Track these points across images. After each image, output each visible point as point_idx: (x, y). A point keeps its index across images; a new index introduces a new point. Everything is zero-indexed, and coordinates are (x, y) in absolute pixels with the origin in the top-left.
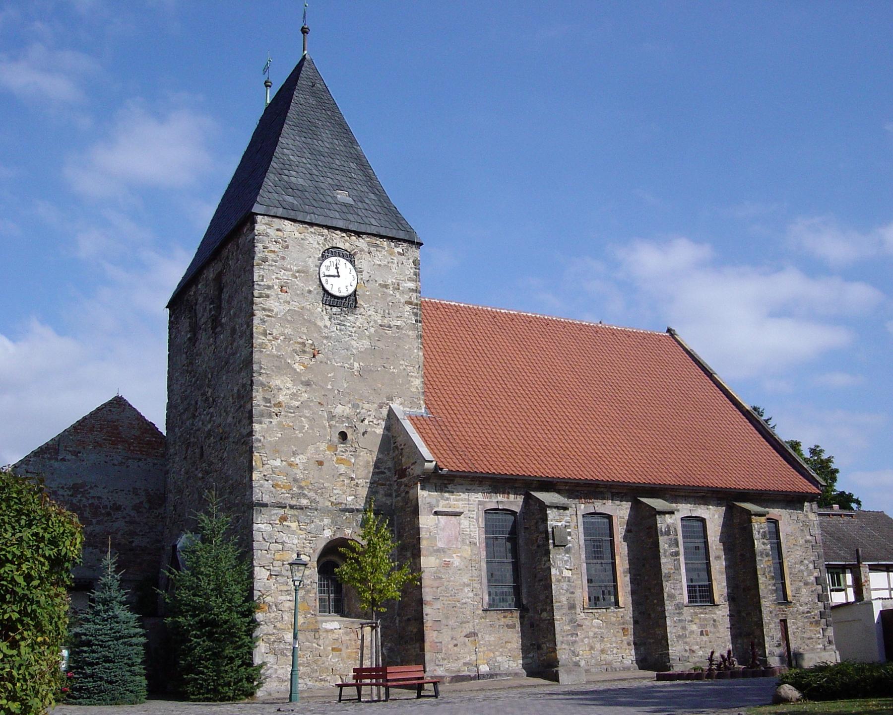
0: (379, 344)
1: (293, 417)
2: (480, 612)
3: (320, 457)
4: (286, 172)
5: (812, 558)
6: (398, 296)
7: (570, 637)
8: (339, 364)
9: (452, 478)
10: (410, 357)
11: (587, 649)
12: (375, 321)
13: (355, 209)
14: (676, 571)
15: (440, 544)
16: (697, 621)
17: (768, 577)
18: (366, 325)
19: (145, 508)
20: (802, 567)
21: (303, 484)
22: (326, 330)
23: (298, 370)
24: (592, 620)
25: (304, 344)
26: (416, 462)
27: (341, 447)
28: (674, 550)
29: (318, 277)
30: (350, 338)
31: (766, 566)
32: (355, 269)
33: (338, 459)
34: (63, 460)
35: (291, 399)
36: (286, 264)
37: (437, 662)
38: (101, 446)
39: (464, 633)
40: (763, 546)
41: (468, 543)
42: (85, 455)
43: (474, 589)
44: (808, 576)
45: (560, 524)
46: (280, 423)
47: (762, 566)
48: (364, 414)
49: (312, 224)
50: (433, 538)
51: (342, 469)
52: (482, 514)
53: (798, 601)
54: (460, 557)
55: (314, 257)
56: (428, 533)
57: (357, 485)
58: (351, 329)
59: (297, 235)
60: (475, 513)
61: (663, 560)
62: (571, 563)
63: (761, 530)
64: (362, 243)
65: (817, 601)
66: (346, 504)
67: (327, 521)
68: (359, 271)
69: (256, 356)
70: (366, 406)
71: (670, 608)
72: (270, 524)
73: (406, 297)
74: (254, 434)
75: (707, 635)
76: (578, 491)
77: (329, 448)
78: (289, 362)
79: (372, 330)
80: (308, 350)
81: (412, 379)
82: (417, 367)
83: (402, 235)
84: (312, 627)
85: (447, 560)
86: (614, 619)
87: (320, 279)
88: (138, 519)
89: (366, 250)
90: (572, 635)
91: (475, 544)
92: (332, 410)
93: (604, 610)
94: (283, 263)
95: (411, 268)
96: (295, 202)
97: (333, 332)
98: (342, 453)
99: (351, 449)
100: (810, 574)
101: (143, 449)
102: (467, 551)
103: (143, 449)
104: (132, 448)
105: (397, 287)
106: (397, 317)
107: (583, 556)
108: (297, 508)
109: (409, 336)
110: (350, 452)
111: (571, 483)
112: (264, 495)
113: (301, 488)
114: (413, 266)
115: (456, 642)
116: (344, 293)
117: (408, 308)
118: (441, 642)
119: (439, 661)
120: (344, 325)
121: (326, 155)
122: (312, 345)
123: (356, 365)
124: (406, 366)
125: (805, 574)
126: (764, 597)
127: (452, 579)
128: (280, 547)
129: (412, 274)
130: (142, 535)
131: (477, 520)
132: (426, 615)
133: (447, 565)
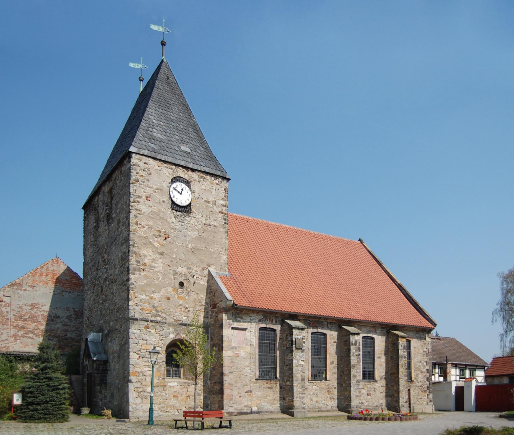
0: (204, 235)
1: (153, 272)
2: (254, 380)
3: (168, 295)
5: (426, 360)
6: (215, 208)
8: (180, 244)
9: (242, 310)
10: (221, 243)
11: (309, 400)
12: (202, 222)
15: (234, 345)
16: (366, 388)
18: (196, 223)
20: (421, 364)
21: (158, 309)
22: (173, 224)
23: (156, 246)
24: (313, 386)
25: (160, 232)
26: (222, 300)
27: (180, 290)
28: (358, 353)
30: (187, 230)
32: (191, 190)
33: (178, 297)
35: (152, 262)
37: (230, 405)
39: (245, 391)
41: (249, 344)
43: (252, 369)
44: (423, 368)
45: (299, 337)
46: (145, 275)
48: (194, 273)
50: (230, 341)
51: (181, 302)
52: (257, 330)
53: (417, 380)
54: (245, 352)
56: (228, 339)
57: (189, 311)
58: (187, 225)
61: (352, 358)
62: (304, 357)
64: (195, 176)
65: (426, 381)
66: (182, 321)
67: (171, 329)
68: (193, 192)
70: (195, 268)
72: (139, 330)
73: (220, 209)
75: (370, 395)
76: (309, 320)
77: (174, 290)
78: (151, 241)
79: (200, 226)
80: (162, 235)
81: (222, 256)
82: (225, 249)
83: (218, 173)
84: (162, 384)
85: (238, 353)
86: (323, 386)
87: (170, 194)
89: (197, 180)
91: (253, 345)
92: (176, 270)
93: (319, 382)
95: (223, 193)
97: (177, 226)
98: (180, 294)
99: (186, 291)
100: (424, 367)
102: (248, 349)
105: (215, 203)
106: (214, 220)
107: (310, 354)
108: (154, 322)
110: (186, 293)
111: (306, 316)
112: (136, 314)
113: (157, 311)
114: (224, 192)
115: (240, 395)
116: (184, 204)
117: (220, 215)
118: (232, 395)
119: (231, 404)
120: (183, 222)
122: (165, 232)
123: (190, 245)
124: (218, 248)
125: (422, 367)
127: (239, 363)
128: (145, 342)
129: (224, 196)
131: (255, 333)
132: (225, 381)
133: (237, 355)
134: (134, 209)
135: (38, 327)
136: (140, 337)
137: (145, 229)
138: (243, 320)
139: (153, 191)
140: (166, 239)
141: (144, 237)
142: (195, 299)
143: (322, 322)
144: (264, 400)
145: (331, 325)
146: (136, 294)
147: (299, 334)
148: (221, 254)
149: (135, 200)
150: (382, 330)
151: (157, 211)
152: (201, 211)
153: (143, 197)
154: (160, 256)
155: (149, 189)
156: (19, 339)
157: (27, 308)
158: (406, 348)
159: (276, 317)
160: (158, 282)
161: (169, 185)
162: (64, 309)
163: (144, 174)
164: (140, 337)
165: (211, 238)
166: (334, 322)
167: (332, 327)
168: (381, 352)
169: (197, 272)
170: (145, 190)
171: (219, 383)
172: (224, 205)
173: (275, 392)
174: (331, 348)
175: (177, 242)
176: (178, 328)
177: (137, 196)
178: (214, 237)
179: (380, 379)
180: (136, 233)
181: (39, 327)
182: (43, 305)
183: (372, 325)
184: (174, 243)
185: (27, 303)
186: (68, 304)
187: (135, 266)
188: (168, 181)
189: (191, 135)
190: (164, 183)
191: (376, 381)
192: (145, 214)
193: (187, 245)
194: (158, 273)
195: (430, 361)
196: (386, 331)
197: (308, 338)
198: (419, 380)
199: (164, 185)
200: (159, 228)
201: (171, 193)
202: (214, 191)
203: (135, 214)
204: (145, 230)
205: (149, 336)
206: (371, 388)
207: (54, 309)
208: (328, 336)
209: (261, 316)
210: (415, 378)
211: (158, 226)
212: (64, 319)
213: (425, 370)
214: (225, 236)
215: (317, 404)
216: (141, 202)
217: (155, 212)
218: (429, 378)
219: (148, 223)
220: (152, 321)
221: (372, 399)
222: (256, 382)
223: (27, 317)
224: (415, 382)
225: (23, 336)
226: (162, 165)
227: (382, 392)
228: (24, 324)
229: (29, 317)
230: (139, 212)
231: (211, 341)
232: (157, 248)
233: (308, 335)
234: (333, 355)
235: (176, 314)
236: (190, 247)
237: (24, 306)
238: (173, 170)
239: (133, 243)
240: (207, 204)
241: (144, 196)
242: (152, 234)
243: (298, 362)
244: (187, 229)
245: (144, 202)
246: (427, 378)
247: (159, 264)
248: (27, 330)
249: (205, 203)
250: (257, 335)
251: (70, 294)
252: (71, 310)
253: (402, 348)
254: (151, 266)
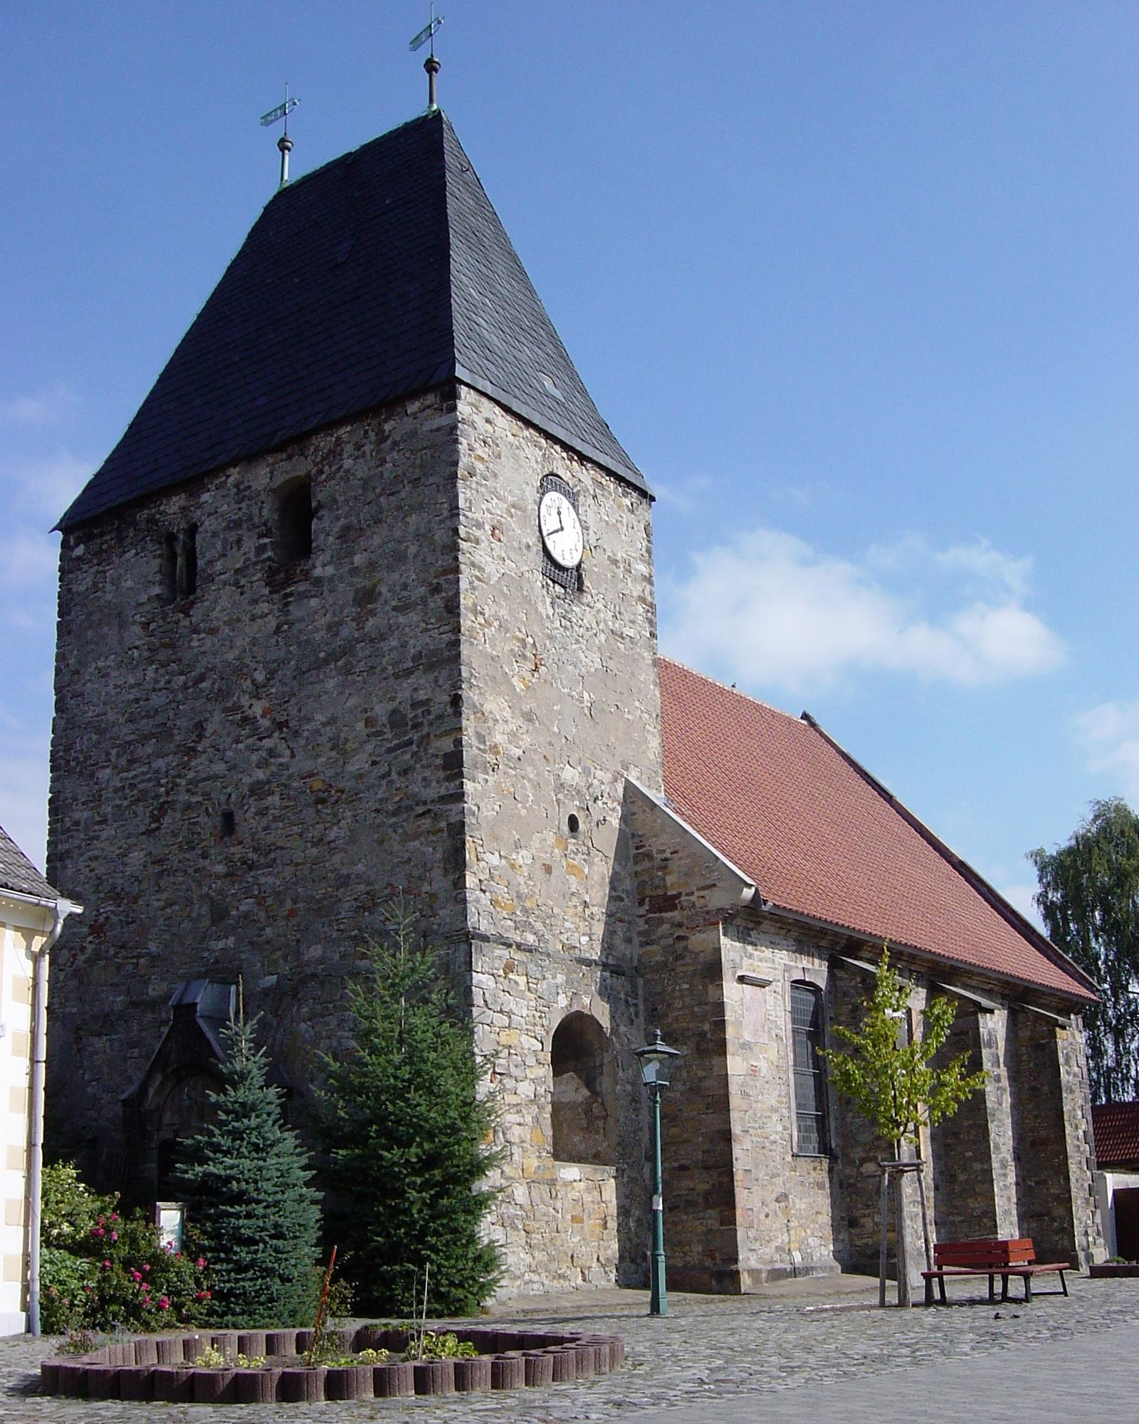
26: (714, 885)
49: (528, 423)
52: (788, 985)
60: (779, 984)
64: (587, 476)
69: (465, 650)
72: (493, 975)
74: (466, 799)
84: (548, 1176)
108: (524, 950)
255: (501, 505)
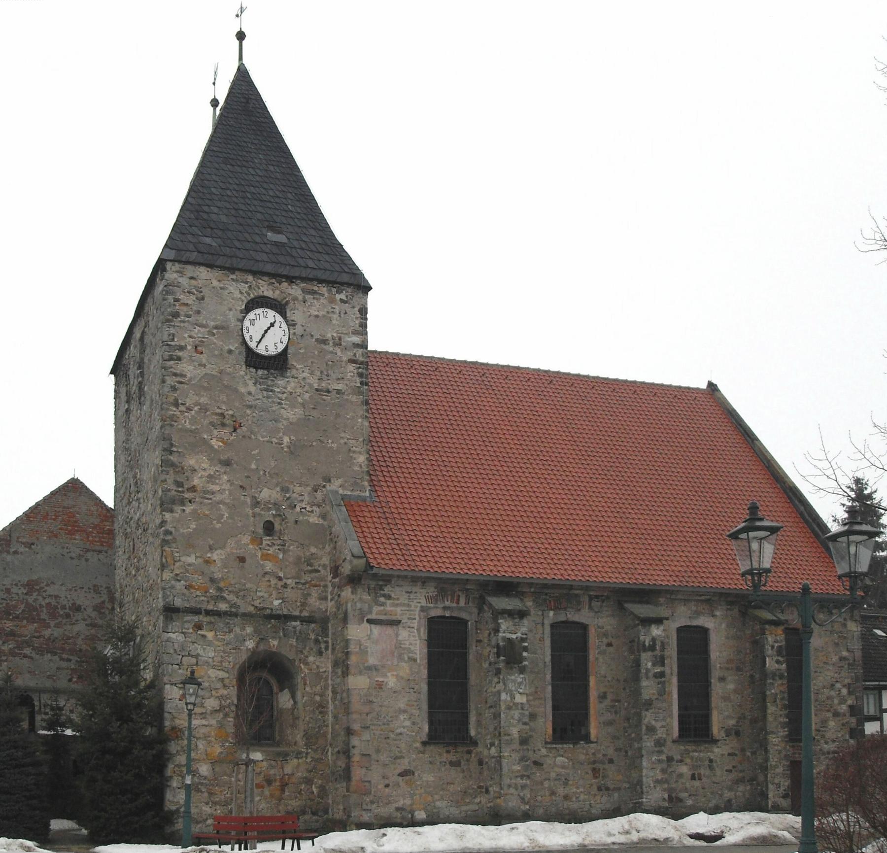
0: (315, 413)
1: (210, 504)
2: (418, 745)
3: (241, 553)
4: (206, 208)
5: (847, 681)
6: (339, 353)
7: (519, 779)
8: (265, 439)
9: (388, 578)
10: (353, 428)
11: (547, 794)
12: (311, 385)
13: (288, 249)
14: (660, 698)
15: (372, 661)
16: (688, 760)
17: (779, 706)
18: (299, 390)
19: (108, 608)
20: (833, 693)
21: (222, 585)
22: (250, 398)
23: (216, 447)
24: (555, 757)
25: (222, 415)
27: (267, 540)
28: (658, 669)
29: (240, 333)
30: (279, 406)
31: (778, 692)
32: (287, 322)
33: (262, 555)
34: (16, 552)
35: (208, 482)
36: (201, 319)
37: (364, 807)
38: (56, 536)
39: (398, 771)
40: (777, 665)
41: (406, 659)
42: (39, 547)
43: (413, 717)
44: (840, 703)
45: (514, 636)
46: (194, 511)
47: (773, 691)
48: (296, 499)
50: (363, 652)
51: (269, 566)
52: (424, 622)
53: (823, 736)
54: (397, 676)
55: (236, 310)
56: (358, 647)
57: (285, 586)
58: (280, 395)
59: (215, 283)
60: (416, 621)
61: (644, 683)
62: (525, 686)
63: (776, 645)
64: (295, 291)
65: (847, 737)
66: (272, 609)
67: (249, 630)
68: (291, 324)
70: (298, 489)
71: (648, 744)
73: (350, 354)
75: (700, 779)
76: (546, 594)
77: (253, 541)
78: (206, 437)
79: (307, 396)
80: (227, 422)
81: (355, 456)
82: (361, 440)
83: (345, 278)
85: (381, 680)
86: (582, 757)
87: (243, 335)
88: (100, 622)
89: (300, 298)
90: (522, 777)
91: (415, 660)
92: (257, 495)
93: (571, 746)
94: (198, 318)
95: (357, 318)
96: (214, 244)
97: (259, 399)
98: (267, 548)
99: (279, 542)
100: (843, 701)
101: (103, 540)
102: (405, 669)
103: (103, 540)
104: (90, 538)
105: (338, 343)
106: (338, 379)
107: (549, 677)
109: (352, 402)
110: (278, 545)
111: (537, 584)
112: (175, 598)
113: (220, 589)
114: (359, 315)
115: (387, 782)
116: (273, 351)
117: (351, 367)
118: (369, 782)
119: (367, 805)
120: (272, 391)
121: (257, 184)
122: (232, 416)
123: (286, 440)
124: (348, 439)
125: (836, 701)
126: (772, 733)
127: (385, 703)
128: (194, 661)
129: (357, 326)
130: (105, 640)
131: (418, 630)
132: (353, 747)
133: (380, 686)
134: (170, 374)
135: (40, 632)
136: (184, 650)
137: (193, 412)
138: (392, 601)
139: (209, 331)
140: (235, 430)
141: (191, 431)
142: (299, 558)
143: (577, 596)
144: (441, 793)
145: (599, 604)
146: (176, 554)
147: (513, 628)
148: (354, 452)
149: (172, 355)
150: (728, 609)
151: (216, 374)
152: (310, 364)
153: (189, 347)
154: (225, 467)
155: (200, 329)
156: (6, 661)
157: (20, 592)
158: (784, 653)
159: (467, 590)
160: (220, 525)
161: (240, 316)
162: (89, 588)
163: (190, 300)
164: (184, 650)
165: (332, 418)
166: (606, 594)
167: (601, 607)
168: (727, 666)
169: (301, 498)
170: (193, 334)
171: (344, 753)
172: (358, 344)
173: (466, 773)
174: (601, 660)
175: (258, 435)
176: (262, 627)
177: (176, 348)
178: (338, 416)
179: (724, 735)
180: (176, 424)
181: (43, 633)
182: (49, 582)
183: (703, 598)
184: (253, 437)
185: (19, 581)
186: (96, 578)
187: (173, 493)
188: (239, 308)
189: (289, 206)
190: (231, 313)
191: (715, 742)
192: (193, 382)
193: (281, 439)
194: (221, 506)
195: (858, 684)
196: (740, 611)
197: (543, 638)
198: (829, 735)
199: (230, 319)
200: (221, 409)
201: (245, 332)
202: (335, 316)
203: (173, 384)
204: (192, 416)
205: (202, 646)
206: (701, 759)
207: (70, 590)
208: (592, 633)
209: (432, 589)
210: (819, 731)
211: (219, 404)
212: (90, 610)
213: (844, 708)
214: (361, 411)
215: (566, 804)
216: (185, 358)
217: (213, 375)
218: (855, 729)
219: (200, 399)
220: (208, 613)
221: (703, 788)
222: (422, 749)
223: (20, 611)
224: (818, 741)
225: (12, 653)
226: (225, 278)
227: (730, 771)
228: (15, 626)
229: (23, 611)
230: (181, 380)
231: (333, 653)
232: (216, 451)
233: (543, 630)
234: (605, 677)
235: (259, 594)
236: (285, 444)
237: (14, 586)
238: (249, 284)
239: (169, 446)
240: (323, 346)
241: (190, 345)
242: (206, 422)
243: (513, 697)
244: (279, 403)
245: (191, 356)
246: (851, 729)
247: (221, 485)
248: (20, 639)
249: (319, 346)
250: (424, 635)
251: (101, 556)
252: (102, 592)
253: (775, 653)
254: (205, 492)
255: (202, 330)
